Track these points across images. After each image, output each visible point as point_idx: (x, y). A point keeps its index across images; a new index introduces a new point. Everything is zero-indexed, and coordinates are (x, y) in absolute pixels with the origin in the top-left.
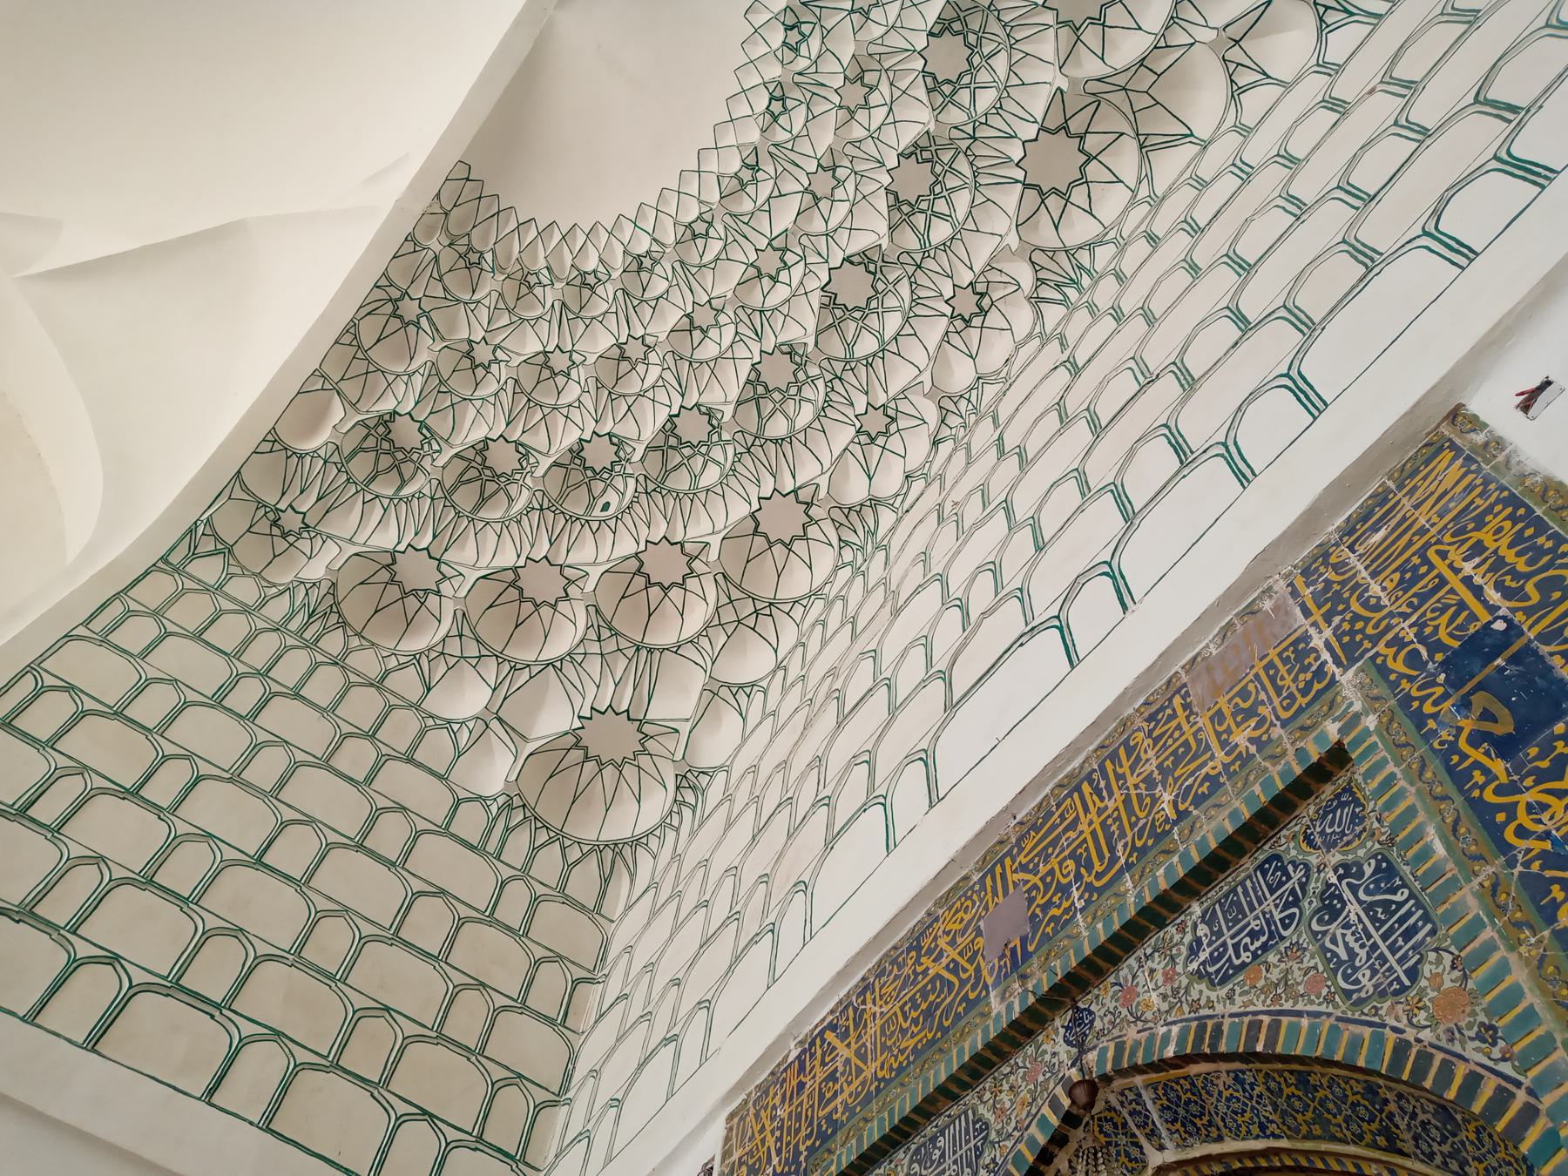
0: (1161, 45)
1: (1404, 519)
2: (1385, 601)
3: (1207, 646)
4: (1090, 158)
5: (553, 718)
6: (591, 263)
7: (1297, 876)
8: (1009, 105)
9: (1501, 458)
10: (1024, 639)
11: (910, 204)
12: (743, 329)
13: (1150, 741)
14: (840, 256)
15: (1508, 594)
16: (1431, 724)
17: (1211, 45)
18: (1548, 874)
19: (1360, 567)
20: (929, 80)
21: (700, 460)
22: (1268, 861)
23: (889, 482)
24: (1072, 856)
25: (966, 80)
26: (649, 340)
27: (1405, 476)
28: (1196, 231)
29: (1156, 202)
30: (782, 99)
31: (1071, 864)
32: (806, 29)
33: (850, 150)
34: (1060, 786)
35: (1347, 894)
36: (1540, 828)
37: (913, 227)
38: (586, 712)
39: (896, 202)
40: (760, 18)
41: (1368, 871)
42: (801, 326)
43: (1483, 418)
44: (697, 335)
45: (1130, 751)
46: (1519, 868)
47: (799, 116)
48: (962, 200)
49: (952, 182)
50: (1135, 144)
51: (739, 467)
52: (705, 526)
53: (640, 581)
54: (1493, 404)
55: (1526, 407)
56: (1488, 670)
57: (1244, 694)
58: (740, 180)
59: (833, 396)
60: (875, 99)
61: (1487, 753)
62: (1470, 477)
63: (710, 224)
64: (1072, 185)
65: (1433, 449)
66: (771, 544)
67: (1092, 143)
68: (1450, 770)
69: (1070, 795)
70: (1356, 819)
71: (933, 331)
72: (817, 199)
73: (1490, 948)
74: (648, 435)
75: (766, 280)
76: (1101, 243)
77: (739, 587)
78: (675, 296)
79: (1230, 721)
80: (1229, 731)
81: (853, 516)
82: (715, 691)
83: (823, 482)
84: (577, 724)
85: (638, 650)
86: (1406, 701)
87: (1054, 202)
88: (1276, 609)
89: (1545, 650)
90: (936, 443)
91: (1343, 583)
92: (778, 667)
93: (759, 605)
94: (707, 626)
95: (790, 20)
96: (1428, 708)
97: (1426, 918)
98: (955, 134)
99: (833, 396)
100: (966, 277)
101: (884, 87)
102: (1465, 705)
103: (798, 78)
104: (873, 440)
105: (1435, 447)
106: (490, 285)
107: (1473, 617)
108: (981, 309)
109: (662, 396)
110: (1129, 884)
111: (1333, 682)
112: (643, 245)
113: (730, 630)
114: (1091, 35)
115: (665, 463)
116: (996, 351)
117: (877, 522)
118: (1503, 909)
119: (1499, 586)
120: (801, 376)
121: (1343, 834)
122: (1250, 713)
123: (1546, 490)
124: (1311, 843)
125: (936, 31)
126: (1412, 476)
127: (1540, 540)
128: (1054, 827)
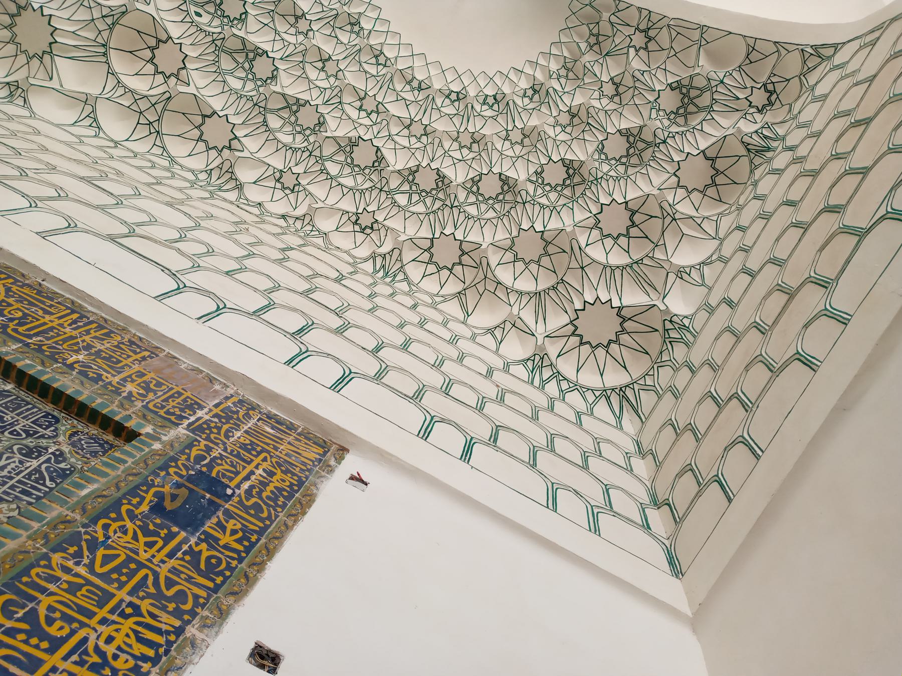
0: (508, 290)
1: (281, 439)
2: (232, 440)
3: (185, 363)
4: (451, 270)
7: (48, 432)
8: (471, 222)
9: (323, 474)
10: (167, 271)
11: (413, 180)
12: (328, 92)
13: (116, 343)
14: (380, 145)
15: (249, 492)
16: (163, 473)
17: (511, 314)
18: (84, 544)
19: (249, 425)
20: (478, 178)
21: (243, 75)
22: (54, 417)
23: (254, 194)
24: (25, 315)
25: (480, 198)
26: (311, 34)
27: (306, 435)
28: (421, 325)
29: (434, 306)
30: (458, 99)
31: (20, 314)
32: (496, 107)
33: (437, 141)
34: (73, 302)
35: (42, 459)
36: (111, 533)
37: (401, 184)
38: (46, 12)
39: (413, 172)
40: (497, 80)
41: (62, 465)
42: (336, 128)
43: (343, 462)
44: (320, 65)
45: (108, 335)
46: (83, 530)
47: (451, 110)
48: (420, 208)
49: (429, 201)
50: (461, 289)
51: (244, 100)
52: (200, 83)
53: (152, 42)
54: (351, 464)
55: (352, 478)
56: (202, 492)
57: (159, 384)
58: (411, 81)
59: (299, 153)
60: (465, 151)
61: (151, 501)
62: (311, 463)
63: (385, 66)
64: (436, 263)
65: (323, 444)
66: (198, 127)
67: (458, 269)
68: (137, 487)
69: (68, 308)
70: (95, 454)
71: (348, 205)
72: (408, 127)
73: (26, 528)
74: (252, 38)
75: (358, 104)
76: (409, 284)
77: (164, 109)
78: (340, 49)
79: (140, 380)
80: (133, 381)
81: (228, 176)
83: (246, 154)
84: (36, 6)
85: (103, 45)
86: (175, 460)
87: (426, 256)
88: (216, 391)
89: (220, 514)
90: (283, 217)
91: (238, 419)
92: (116, 142)
93: (155, 125)
95: (499, 97)
96: (172, 470)
97: (38, 498)
98: (453, 196)
99: (299, 153)
100: (380, 218)
101: (472, 155)
102: (178, 486)
103: (470, 106)
104: (278, 181)
105: (324, 446)
107: (231, 479)
108: (364, 229)
109: (278, 45)
110: (14, 347)
111: (177, 425)
112: (366, 25)
113: (134, 107)
114: (509, 256)
115: (237, 51)
116: (342, 241)
117: (227, 190)
118: (55, 527)
119: (252, 487)
120: (308, 132)
121: (83, 449)
122: (148, 389)
123: (309, 495)
124: (71, 436)
125: (503, 177)
126: (306, 438)
127: (281, 499)
128: (43, 303)
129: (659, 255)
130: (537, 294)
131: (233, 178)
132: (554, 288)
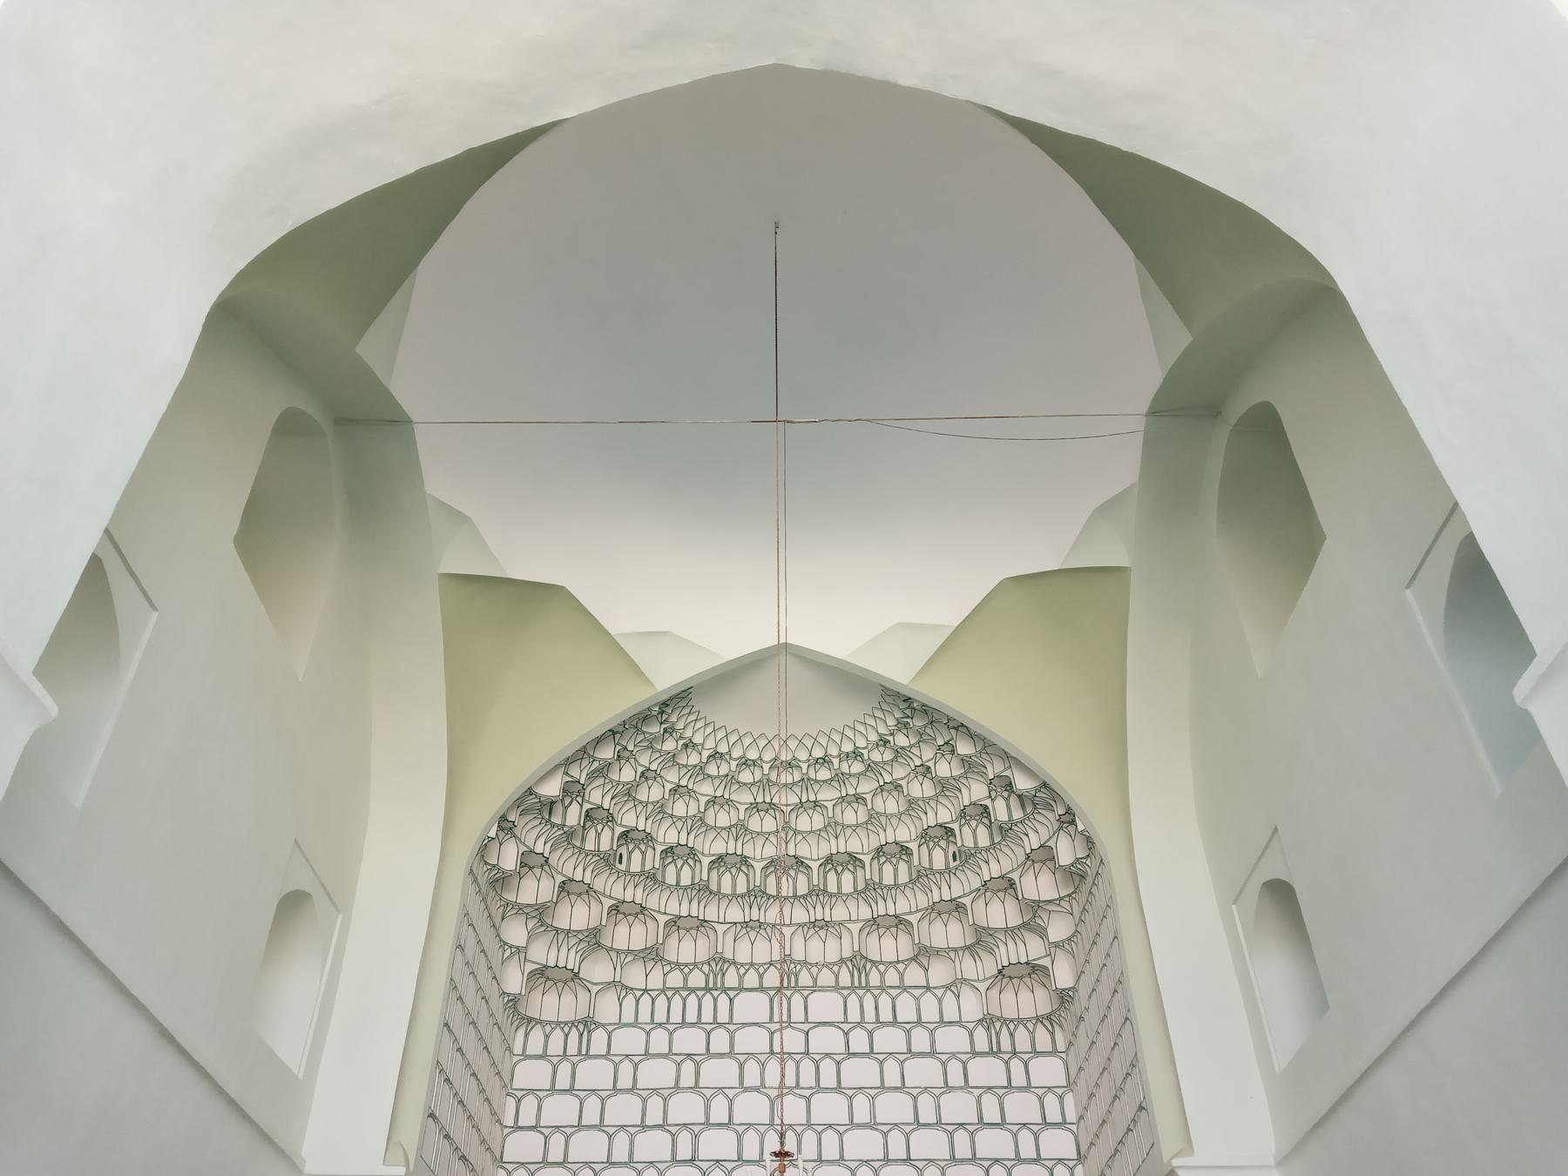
5: (542, 953)
6: (698, 739)
40: (849, 733)
71: (800, 915)
78: (717, 782)
92: (646, 990)
94: (629, 952)
106: (654, 729)
109: (679, 824)
112: (723, 749)
129: (1039, 921)
130: (966, 948)
131: (725, 961)
132: (978, 942)
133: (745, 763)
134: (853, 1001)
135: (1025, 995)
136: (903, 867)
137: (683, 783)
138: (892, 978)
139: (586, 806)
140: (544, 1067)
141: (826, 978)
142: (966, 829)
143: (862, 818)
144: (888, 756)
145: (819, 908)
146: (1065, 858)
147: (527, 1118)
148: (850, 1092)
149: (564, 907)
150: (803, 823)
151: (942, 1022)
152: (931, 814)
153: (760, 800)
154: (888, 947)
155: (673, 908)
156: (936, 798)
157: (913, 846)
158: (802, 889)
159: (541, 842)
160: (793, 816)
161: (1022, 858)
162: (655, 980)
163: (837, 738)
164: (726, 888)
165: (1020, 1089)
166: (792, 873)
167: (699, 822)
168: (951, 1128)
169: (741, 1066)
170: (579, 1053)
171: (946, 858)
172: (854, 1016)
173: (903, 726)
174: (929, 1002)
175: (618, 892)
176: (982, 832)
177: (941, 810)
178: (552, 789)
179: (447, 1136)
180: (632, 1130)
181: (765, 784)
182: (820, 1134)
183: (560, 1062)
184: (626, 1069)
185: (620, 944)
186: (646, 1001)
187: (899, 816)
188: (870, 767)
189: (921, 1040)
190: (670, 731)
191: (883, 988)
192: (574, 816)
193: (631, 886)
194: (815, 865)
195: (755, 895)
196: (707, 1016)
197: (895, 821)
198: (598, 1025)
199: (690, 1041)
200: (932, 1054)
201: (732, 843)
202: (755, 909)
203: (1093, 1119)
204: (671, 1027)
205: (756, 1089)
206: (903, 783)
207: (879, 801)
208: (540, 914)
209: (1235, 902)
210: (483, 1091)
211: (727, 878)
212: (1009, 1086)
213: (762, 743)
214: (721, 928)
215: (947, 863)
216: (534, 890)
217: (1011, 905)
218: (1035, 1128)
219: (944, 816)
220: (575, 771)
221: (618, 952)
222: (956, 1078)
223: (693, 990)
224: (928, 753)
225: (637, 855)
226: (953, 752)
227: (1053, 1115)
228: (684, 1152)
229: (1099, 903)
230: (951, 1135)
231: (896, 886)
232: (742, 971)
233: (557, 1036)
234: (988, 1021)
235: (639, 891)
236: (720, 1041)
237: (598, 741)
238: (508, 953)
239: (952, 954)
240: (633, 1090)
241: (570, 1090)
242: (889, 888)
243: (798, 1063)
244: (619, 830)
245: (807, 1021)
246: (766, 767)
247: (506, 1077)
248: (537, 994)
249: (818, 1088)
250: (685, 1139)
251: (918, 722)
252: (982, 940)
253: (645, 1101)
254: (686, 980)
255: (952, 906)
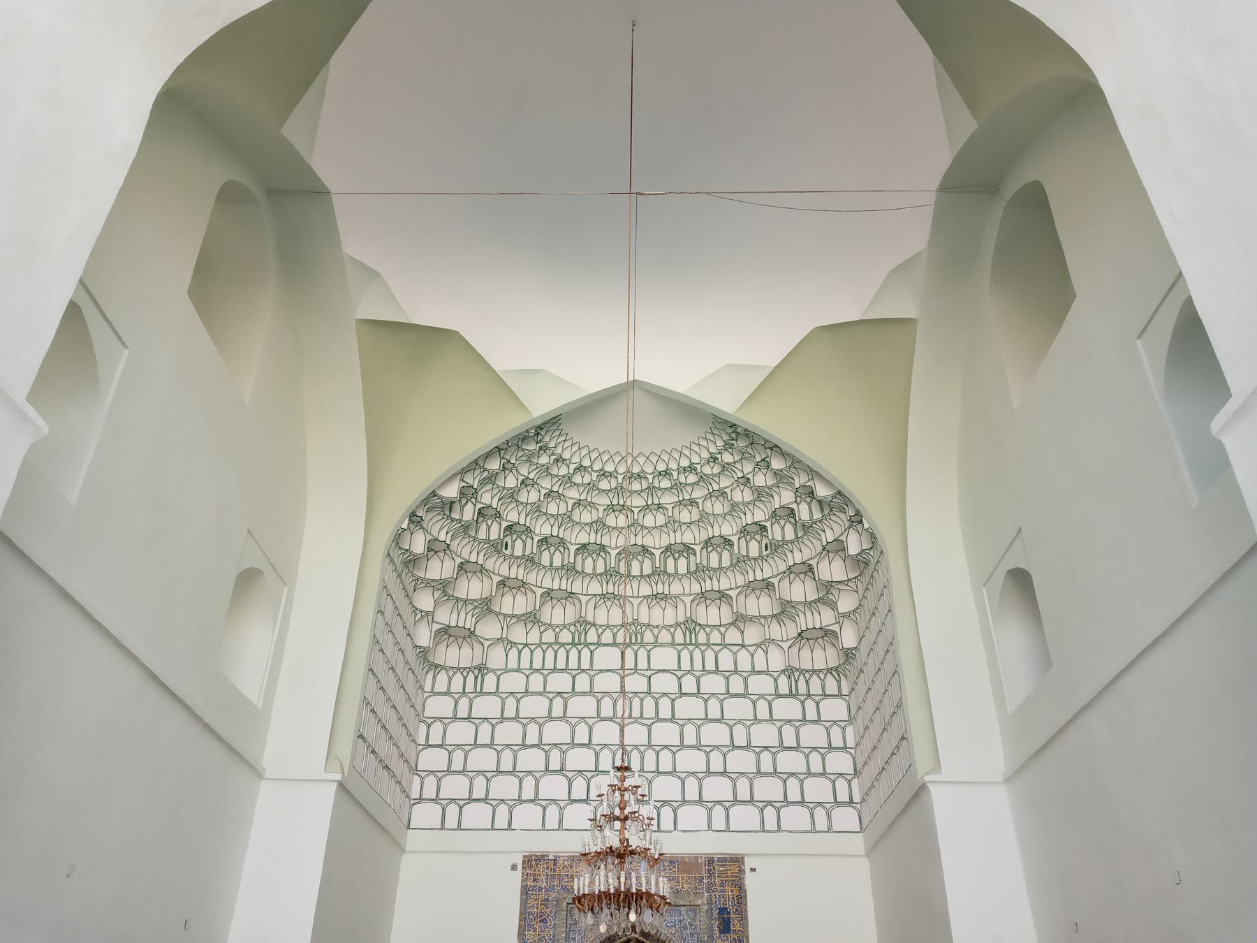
5: (445, 616)
6: (566, 455)
40: (687, 452)
71: (646, 590)
78: (581, 489)
82: (501, 640)
92: (526, 645)
94: (514, 616)
109: (552, 521)
112: (586, 463)
130: (774, 616)
133: (604, 474)
134: (685, 655)
135: (818, 653)
136: (726, 554)
137: (555, 489)
138: (716, 637)
139: (479, 506)
140: (449, 702)
141: (665, 637)
142: (776, 527)
143: (695, 517)
144: (717, 469)
145: (660, 585)
146: (854, 547)
147: (435, 738)
148: (681, 722)
149: (463, 582)
150: (649, 520)
151: (753, 672)
152: (749, 515)
153: (615, 502)
154: (713, 614)
155: (547, 583)
156: (753, 502)
157: (734, 539)
158: (647, 570)
159: (444, 531)
160: (641, 515)
161: (819, 549)
162: (534, 637)
163: (676, 455)
164: (589, 569)
165: (812, 722)
166: (640, 558)
167: (567, 519)
168: (758, 750)
169: (599, 702)
170: (475, 691)
171: (760, 548)
172: (686, 665)
173: (729, 446)
174: (744, 657)
175: (504, 570)
176: (789, 529)
177: (757, 511)
178: (451, 492)
179: (373, 752)
180: (515, 748)
181: (619, 490)
182: (658, 753)
183: (460, 698)
184: (511, 702)
185: (507, 609)
186: (526, 652)
187: (724, 516)
188: (703, 478)
189: (736, 685)
190: (544, 449)
191: (708, 645)
192: (469, 513)
193: (515, 567)
194: (657, 553)
195: (610, 574)
196: (573, 664)
197: (720, 520)
198: (489, 670)
199: (560, 682)
200: (745, 695)
201: (593, 535)
202: (611, 585)
203: (867, 745)
204: (545, 672)
205: (610, 719)
206: (728, 491)
207: (708, 504)
208: (444, 587)
209: (985, 585)
210: (400, 718)
211: (589, 562)
212: (804, 720)
213: (617, 459)
214: (584, 599)
215: (760, 552)
216: (438, 569)
217: (810, 584)
218: (823, 751)
219: (759, 516)
220: (469, 479)
221: (505, 616)
222: (763, 713)
223: (563, 645)
224: (748, 468)
225: (519, 544)
226: (768, 467)
227: (837, 741)
228: (555, 764)
229: (879, 584)
230: (758, 755)
231: (720, 568)
232: (600, 631)
233: (458, 679)
234: (789, 671)
235: (521, 570)
236: (583, 683)
237: (487, 456)
238: (419, 616)
239: (763, 621)
240: (516, 718)
241: (468, 719)
242: (715, 570)
243: (642, 700)
244: (505, 524)
245: (649, 669)
246: (620, 478)
247: (419, 708)
248: (442, 647)
249: (658, 719)
250: (555, 756)
251: (741, 444)
252: (786, 610)
253: (525, 726)
254: (557, 637)
255: (763, 584)
